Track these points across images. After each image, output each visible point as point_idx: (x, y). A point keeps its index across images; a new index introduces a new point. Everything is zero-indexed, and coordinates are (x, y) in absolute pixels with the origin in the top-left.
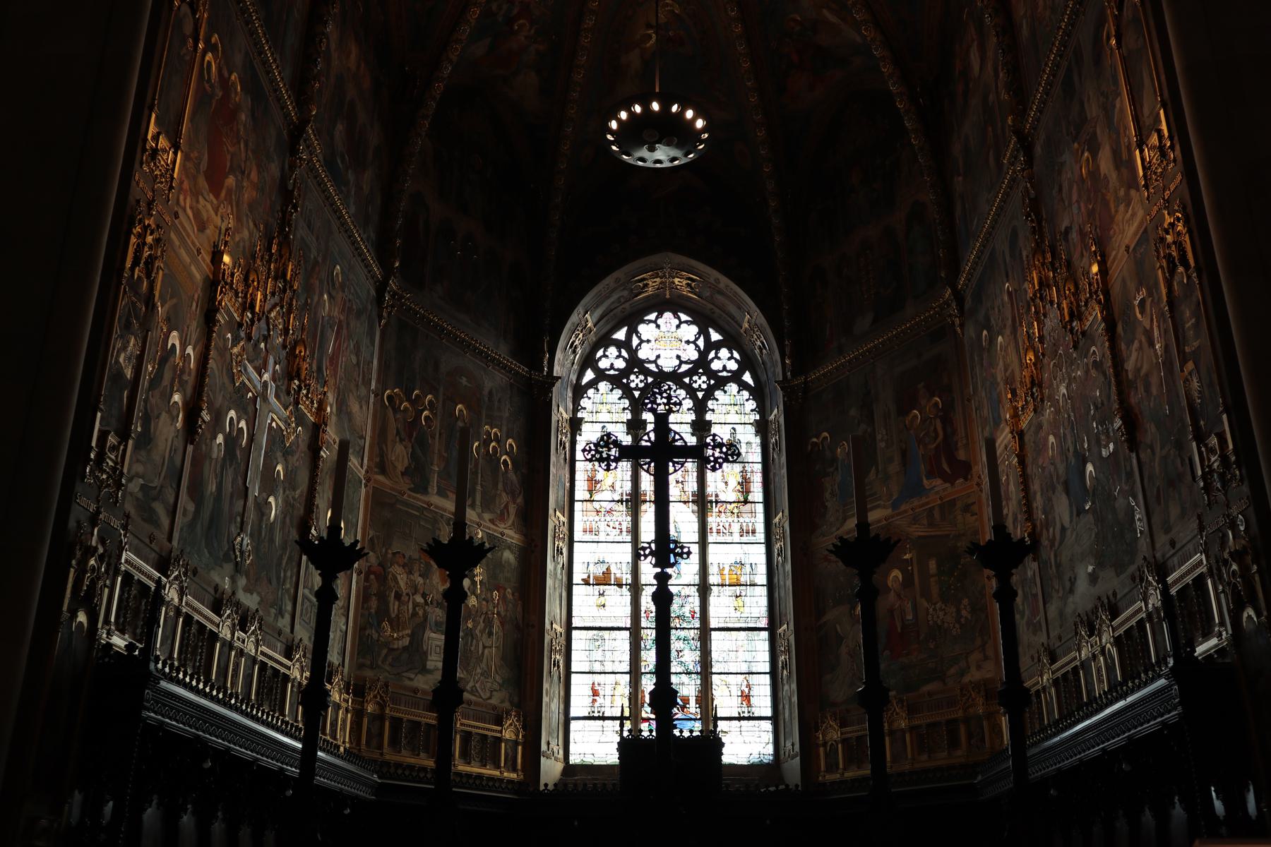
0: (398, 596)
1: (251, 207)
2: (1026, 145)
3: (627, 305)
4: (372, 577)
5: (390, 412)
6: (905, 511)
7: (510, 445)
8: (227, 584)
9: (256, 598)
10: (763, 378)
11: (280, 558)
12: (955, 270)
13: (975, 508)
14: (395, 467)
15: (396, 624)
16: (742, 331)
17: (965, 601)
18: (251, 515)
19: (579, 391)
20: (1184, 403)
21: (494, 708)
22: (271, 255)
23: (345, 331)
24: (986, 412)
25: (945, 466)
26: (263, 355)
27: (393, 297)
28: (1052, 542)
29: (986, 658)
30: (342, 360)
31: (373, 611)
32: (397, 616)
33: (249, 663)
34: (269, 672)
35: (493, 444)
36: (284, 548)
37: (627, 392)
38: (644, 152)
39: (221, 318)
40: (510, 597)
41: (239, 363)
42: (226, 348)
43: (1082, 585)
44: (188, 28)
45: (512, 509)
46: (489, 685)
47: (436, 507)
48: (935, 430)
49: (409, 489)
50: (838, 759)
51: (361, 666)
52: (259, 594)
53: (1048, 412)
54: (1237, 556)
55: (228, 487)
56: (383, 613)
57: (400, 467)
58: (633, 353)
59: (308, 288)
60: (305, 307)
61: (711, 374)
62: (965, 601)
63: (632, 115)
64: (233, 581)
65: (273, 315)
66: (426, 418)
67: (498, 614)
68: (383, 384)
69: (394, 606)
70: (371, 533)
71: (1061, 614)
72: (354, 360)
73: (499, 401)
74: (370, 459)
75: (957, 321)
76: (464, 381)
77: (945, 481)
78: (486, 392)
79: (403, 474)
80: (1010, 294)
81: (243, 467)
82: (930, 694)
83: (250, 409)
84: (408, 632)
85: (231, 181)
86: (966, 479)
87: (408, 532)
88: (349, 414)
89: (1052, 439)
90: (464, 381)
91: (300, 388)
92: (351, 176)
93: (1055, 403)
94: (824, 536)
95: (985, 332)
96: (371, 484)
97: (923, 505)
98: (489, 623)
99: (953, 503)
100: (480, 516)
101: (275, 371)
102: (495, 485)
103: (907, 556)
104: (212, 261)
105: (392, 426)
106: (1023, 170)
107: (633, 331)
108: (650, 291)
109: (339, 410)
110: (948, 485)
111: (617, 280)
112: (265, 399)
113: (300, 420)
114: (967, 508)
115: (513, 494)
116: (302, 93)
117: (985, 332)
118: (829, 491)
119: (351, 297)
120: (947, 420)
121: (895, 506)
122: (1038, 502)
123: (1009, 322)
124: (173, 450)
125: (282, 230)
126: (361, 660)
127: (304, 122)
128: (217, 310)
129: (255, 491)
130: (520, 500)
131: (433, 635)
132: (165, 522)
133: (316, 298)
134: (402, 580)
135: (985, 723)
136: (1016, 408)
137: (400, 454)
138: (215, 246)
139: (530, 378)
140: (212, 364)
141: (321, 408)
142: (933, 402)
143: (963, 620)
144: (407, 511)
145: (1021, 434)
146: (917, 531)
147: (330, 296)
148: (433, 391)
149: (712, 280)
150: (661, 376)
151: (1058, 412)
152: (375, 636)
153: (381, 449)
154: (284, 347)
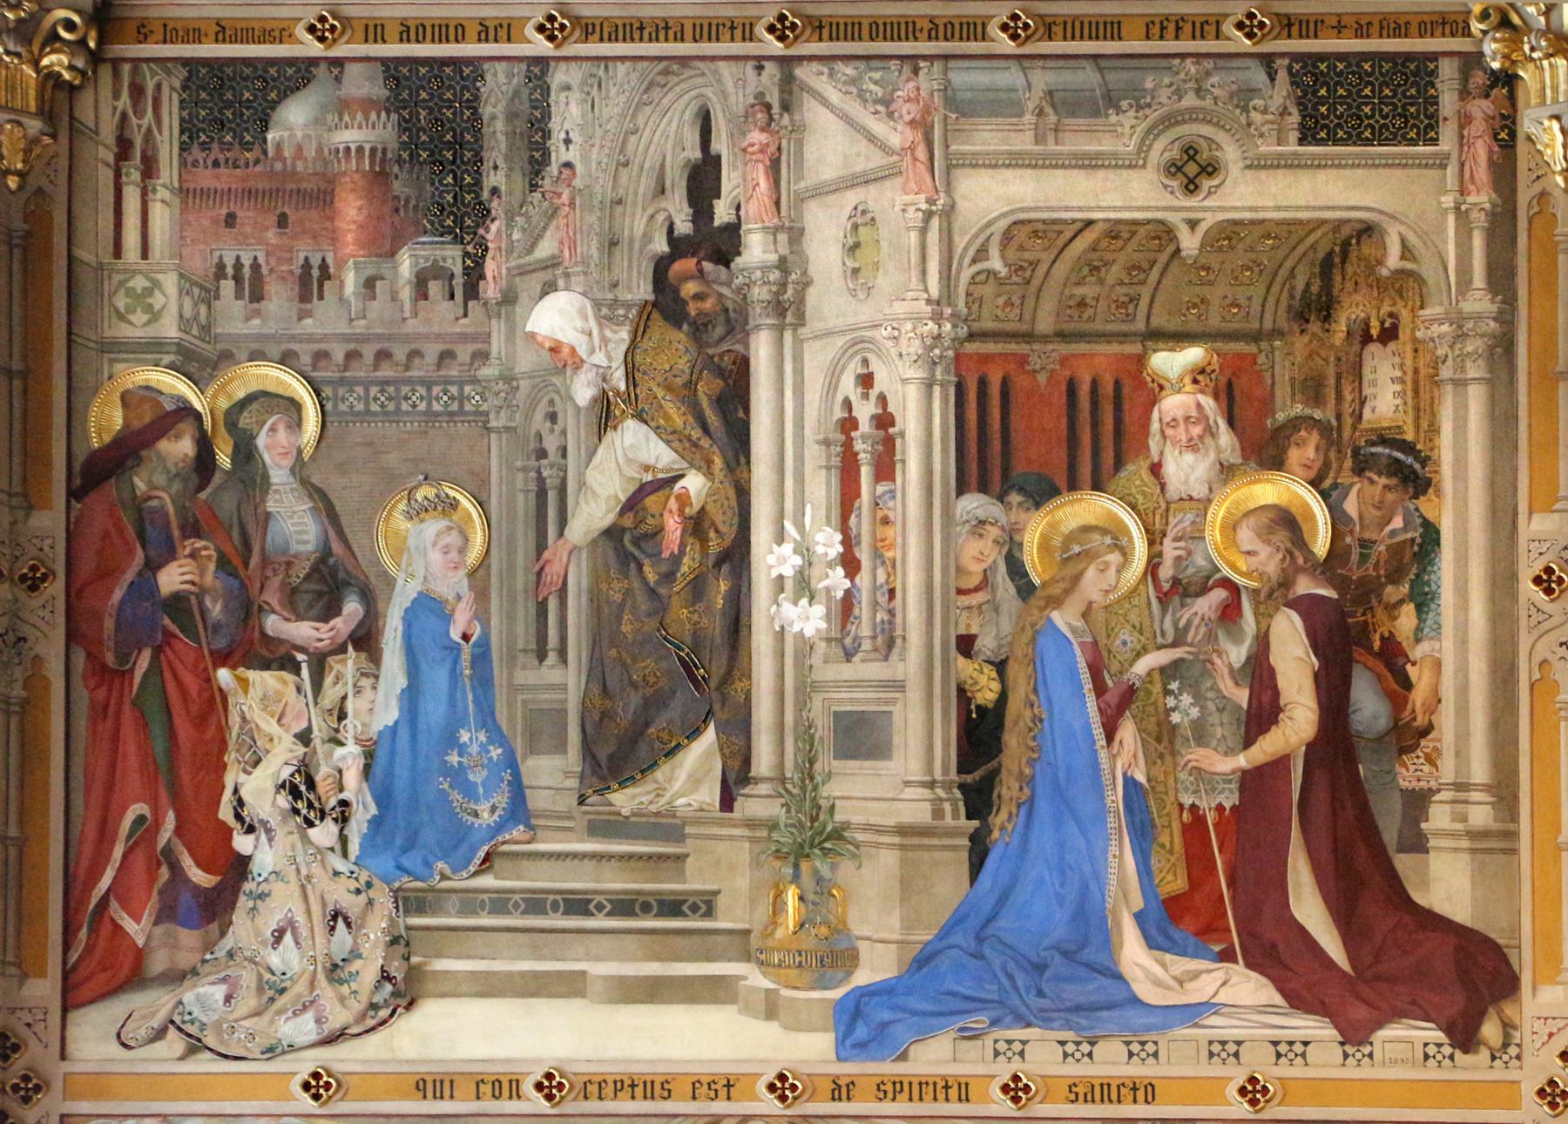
77: (1297, 1000)
86: (1464, 1037)
94: (195, 1046)
118: (280, 760)
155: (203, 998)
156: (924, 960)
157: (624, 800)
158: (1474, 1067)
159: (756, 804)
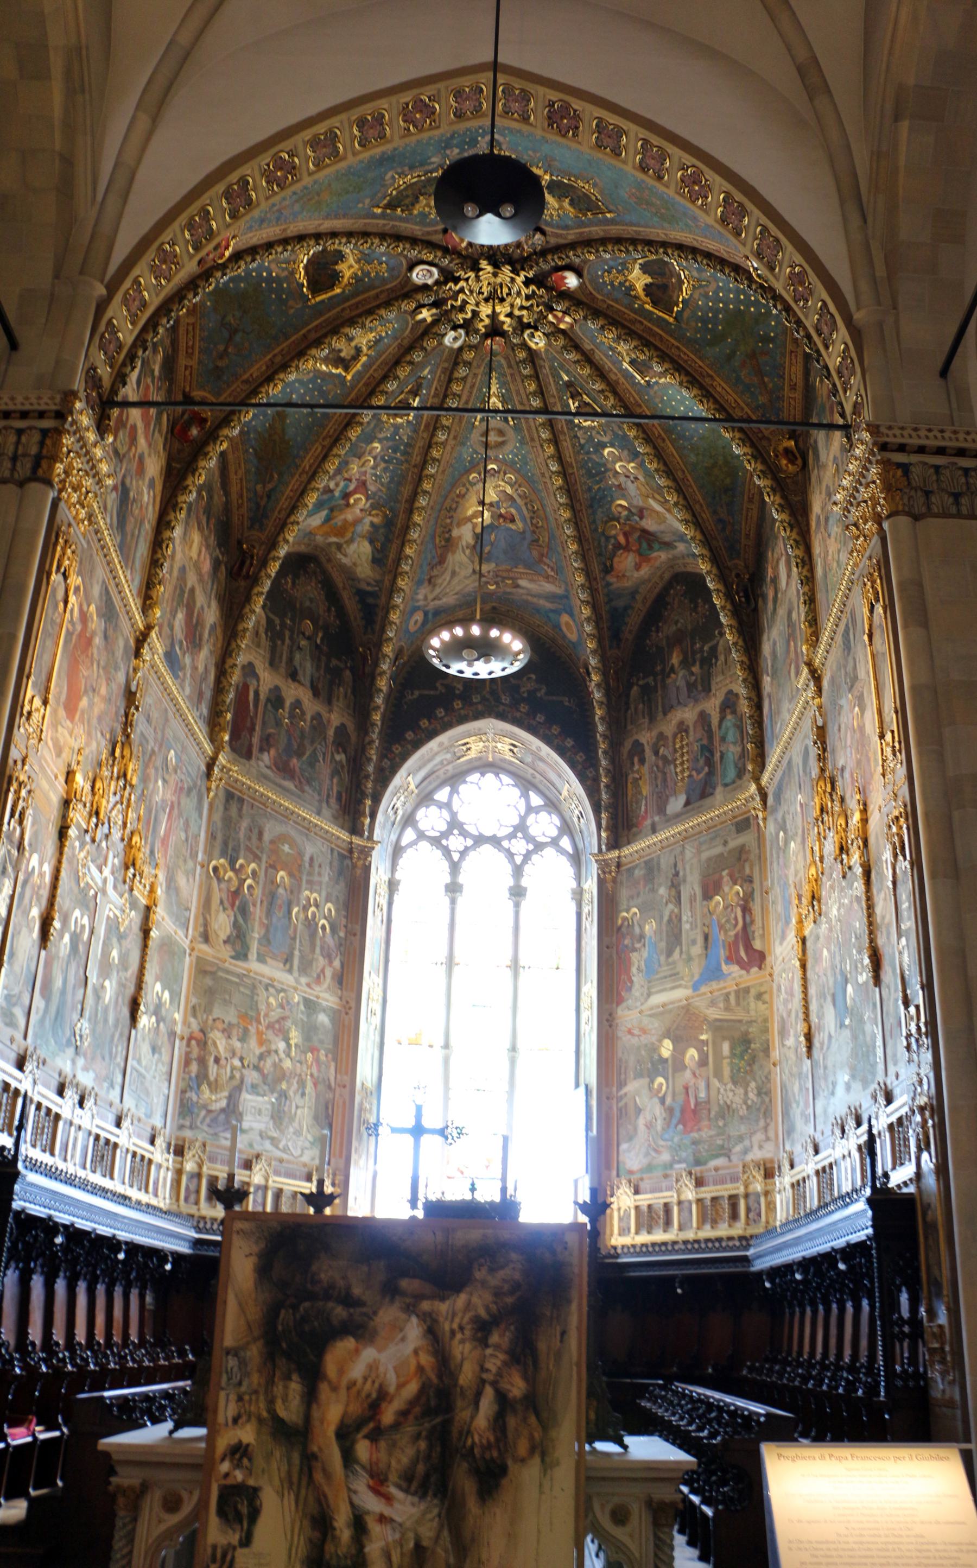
0: (217, 1060)
1: (100, 719)
2: (816, 677)
3: (450, 767)
4: (193, 1042)
5: (215, 882)
6: (704, 994)
7: (330, 910)
8: (67, 1068)
9: (91, 1075)
10: (580, 845)
11: (113, 1036)
12: (762, 766)
13: (766, 997)
14: (217, 936)
15: (215, 1087)
16: (562, 798)
17: (753, 1085)
18: (90, 1000)
19: (397, 851)
20: (898, 971)
21: (305, 1165)
22: (115, 758)
23: (176, 811)
24: (780, 908)
25: (743, 954)
26: (104, 852)
27: (222, 770)
28: (822, 1044)
29: (768, 1139)
30: (173, 839)
31: (193, 1075)
32: (216, 1080)
33: (86, 1135)
34: (102, 1142)
35: (313, 909)
36: (116, 1026)
37: (447, 852)
38: (462, 665)
39: (73, 832)
40: (323, 1058)
41: (84, 866)
42: (74, 855)
43: (840, 1090)
44: (60, 594)
45: (329, 973)
46: (300, 1143)
47: (256, 973)
48: (736, 919)
49: (232, 957)
50: (629, 1223)
51: (181, 1127)
52: (94, 1071)
53: (824, 927)
54: (922, 1109)
55: (71, 980)
56: (202, 1077)
57: (223, 936)
58: (454, 815)
59: (145, 779)
60: (142, 796)
61: (529, 839)
62: (753, 1085)
63: (453, 636)
64: (74, 1062)
65: (114, 813)
66: (250, 887)
67: (312, 1075)
68: (210, 856)
69: (213, 1070)
70: (194, 1001)
71: (825, 1112)
72: (183, 836)
73: (320, 866)
74: (195, 929)
75: (760, 815)
76: (286, 848)
77: (742, 968)
78: (307, 858)
79: (225, 942)
80: (801, 805)
81: (84, 958)
82: (716, 1169)
83: (92, 905)
84: (226, 1094)
85: (84, 703)
86: (760, 968)
87: (227, 997)
88: (177, 890)
89: (825, 952)
90: (286, 848)
91: (134, 875)
92: (187, 660)
93: (829, 921)
95: (782, 834)
96: (195, 954)
97: (720, 989)
98: (302, 1084)
99: (747, 990)
100: (297, 981)
101: (113, 865)
102: (313, 950)
103: (704, 1037)
104: (66, 782)
105: (216, 897)
106: (813, 698)
107: (454, 791)
108: (472, 754)
109: (168, 887)
110: (744, 972)
111: (441, 744)
112: (104, 892)
113: (133, 904)
114: (759, 996)
115: (329, 958)
116: (147, 600)
117: (782, 834)
119: (183, 777)
120: (746, 910)
121: (695, 987)
122: (813, 1007)
123: (800, 832)
124: (30, 959)
125: (125, 730)
126: (181, 1122)
127: (149, 628)
128: (68, 827)
129: (93, 979)
130: (337, 963)
131: (248, 1097)
132: (22, 1022)
133: (151, 786)
134: (222, 1044)
135: (762, 1200)
136: (800, 915)
137: (222, 923)
138: (69, 765)
139: (351, 843)
140: (63, 874)
141: (152, 891)
142: (734, 891)
143: (749, 1102)
144: (227, 980)
145: (804, 940)
146: (714, 1013)
147: (164, 781)
148: (257, 858)
149: (534, 748)
150: (480, 840)
151: (830, 930)
152: (195, 1098)
153: (205, 919)
154: (123, 840)
155: (630, 1002)
156: (701, 975)
157: (670, 960)
158: (762, 972)
159: (684, 956)
